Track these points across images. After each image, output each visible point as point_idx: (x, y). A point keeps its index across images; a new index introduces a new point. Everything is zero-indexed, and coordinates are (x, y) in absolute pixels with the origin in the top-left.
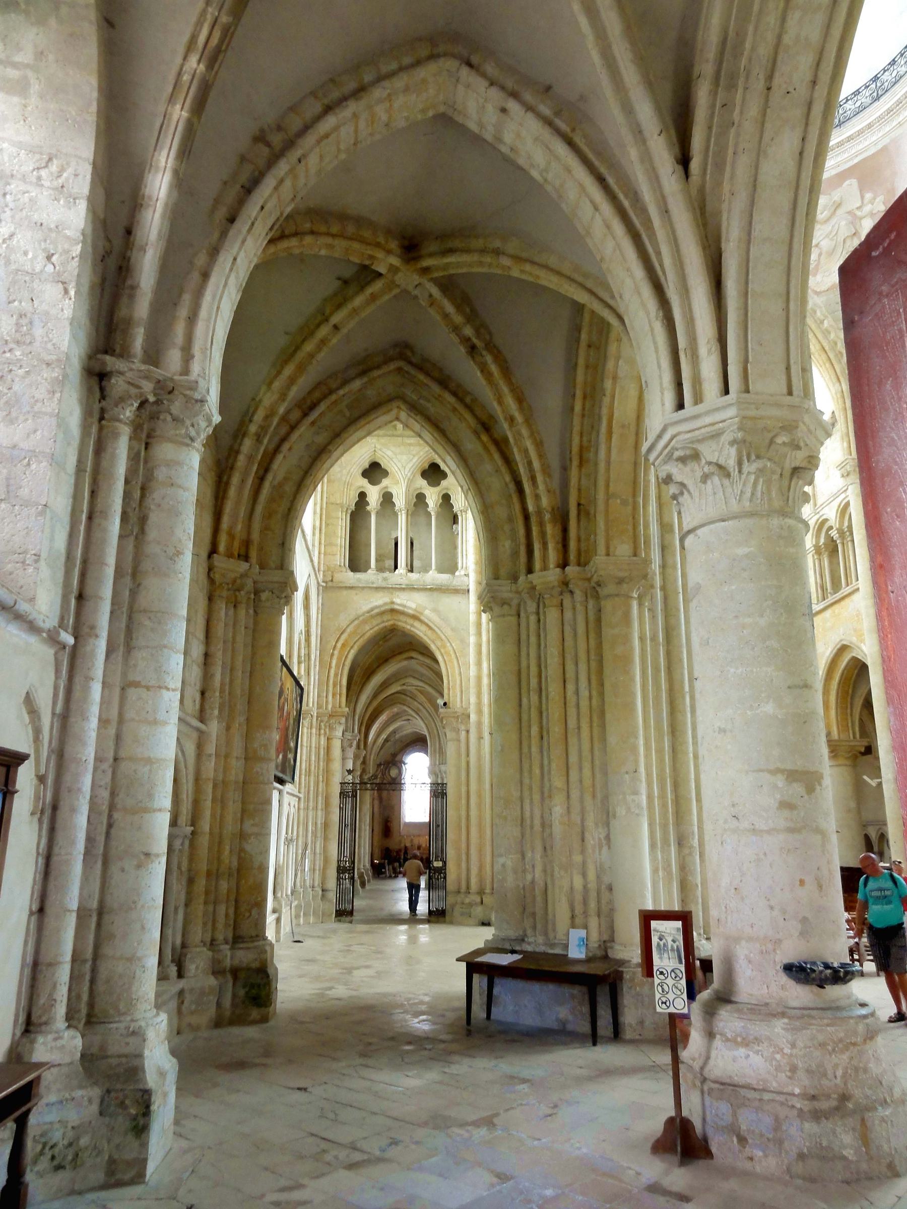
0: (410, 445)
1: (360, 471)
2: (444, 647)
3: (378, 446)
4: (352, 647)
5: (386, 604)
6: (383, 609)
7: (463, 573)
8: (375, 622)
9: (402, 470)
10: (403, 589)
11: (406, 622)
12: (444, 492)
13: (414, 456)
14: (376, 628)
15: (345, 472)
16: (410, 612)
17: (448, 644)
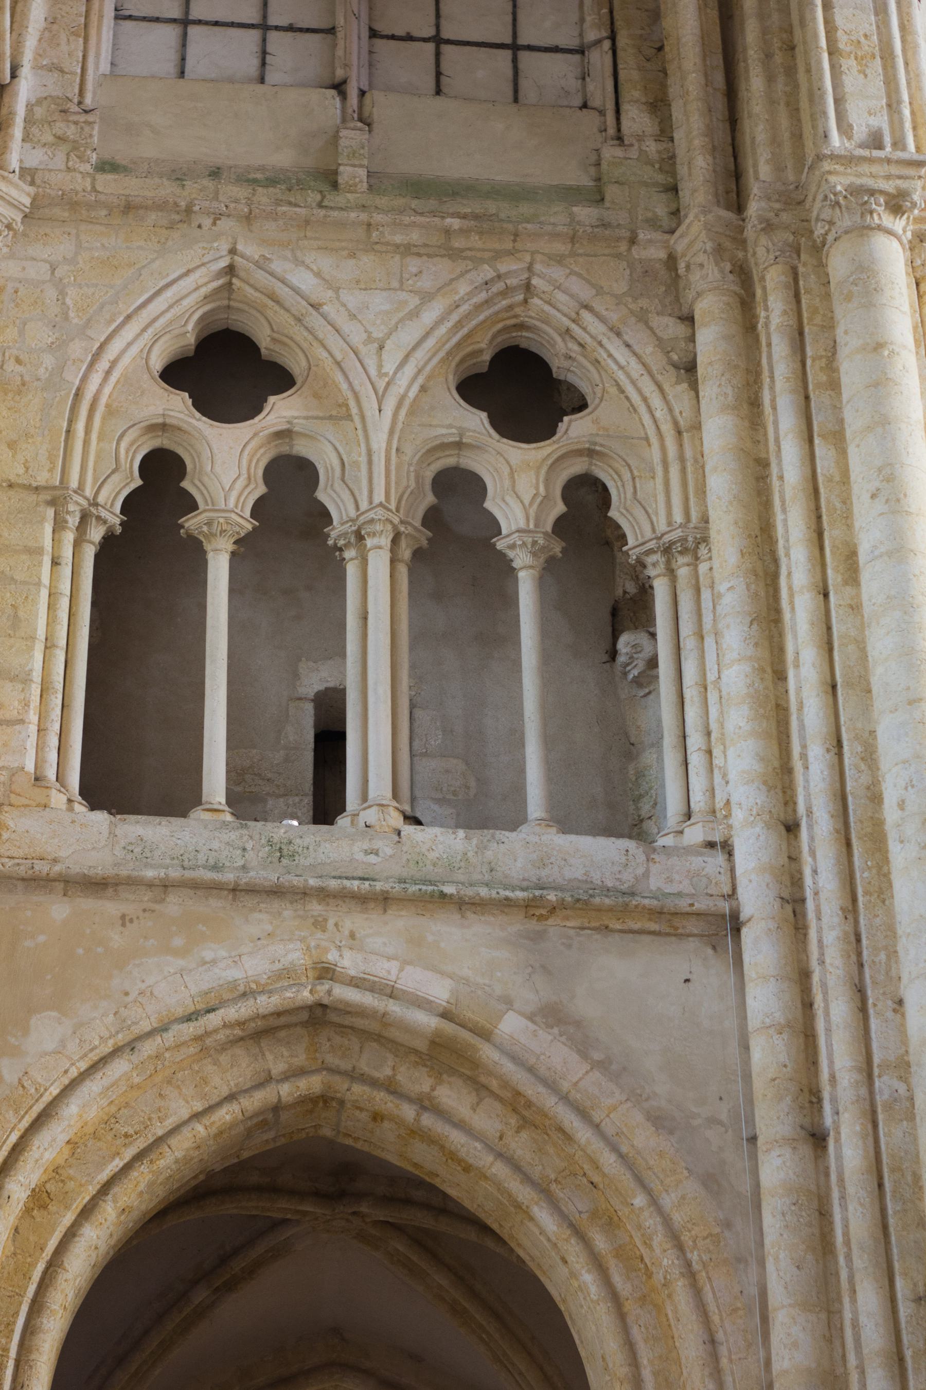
0: (407, 250)
1: (158, 363)
2: (611, 1223)
3: (249, 249)
4: (86, 1213)
5: (286, 974)
6: (265, 1003)
7: (695, 834)
8: (220, 1084)
9: (368, 353)
10: (385, 900)
11: (391, 1087)
12: (577, 467)
13: (427, 297)
14: (226, 1115)
15: (78, 349)
16: (426, 1021)
17: (640, 1200)
